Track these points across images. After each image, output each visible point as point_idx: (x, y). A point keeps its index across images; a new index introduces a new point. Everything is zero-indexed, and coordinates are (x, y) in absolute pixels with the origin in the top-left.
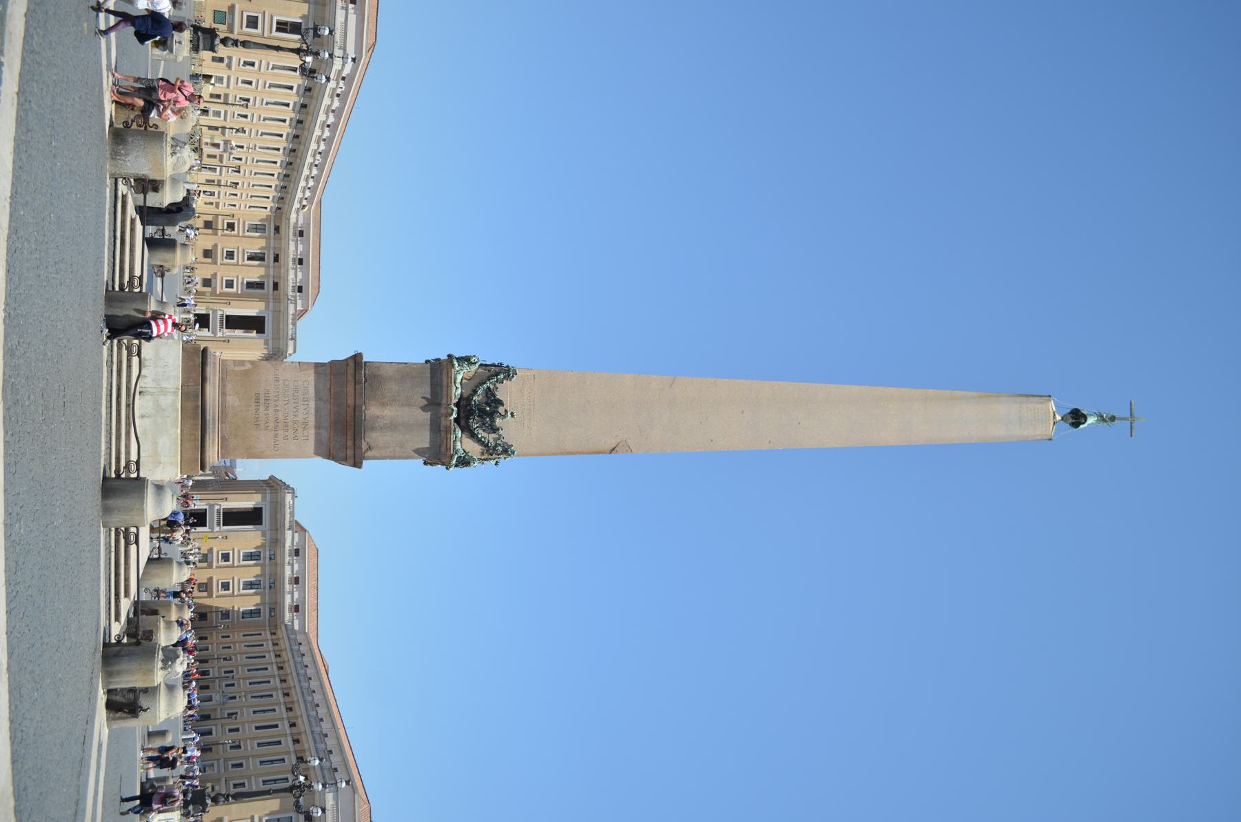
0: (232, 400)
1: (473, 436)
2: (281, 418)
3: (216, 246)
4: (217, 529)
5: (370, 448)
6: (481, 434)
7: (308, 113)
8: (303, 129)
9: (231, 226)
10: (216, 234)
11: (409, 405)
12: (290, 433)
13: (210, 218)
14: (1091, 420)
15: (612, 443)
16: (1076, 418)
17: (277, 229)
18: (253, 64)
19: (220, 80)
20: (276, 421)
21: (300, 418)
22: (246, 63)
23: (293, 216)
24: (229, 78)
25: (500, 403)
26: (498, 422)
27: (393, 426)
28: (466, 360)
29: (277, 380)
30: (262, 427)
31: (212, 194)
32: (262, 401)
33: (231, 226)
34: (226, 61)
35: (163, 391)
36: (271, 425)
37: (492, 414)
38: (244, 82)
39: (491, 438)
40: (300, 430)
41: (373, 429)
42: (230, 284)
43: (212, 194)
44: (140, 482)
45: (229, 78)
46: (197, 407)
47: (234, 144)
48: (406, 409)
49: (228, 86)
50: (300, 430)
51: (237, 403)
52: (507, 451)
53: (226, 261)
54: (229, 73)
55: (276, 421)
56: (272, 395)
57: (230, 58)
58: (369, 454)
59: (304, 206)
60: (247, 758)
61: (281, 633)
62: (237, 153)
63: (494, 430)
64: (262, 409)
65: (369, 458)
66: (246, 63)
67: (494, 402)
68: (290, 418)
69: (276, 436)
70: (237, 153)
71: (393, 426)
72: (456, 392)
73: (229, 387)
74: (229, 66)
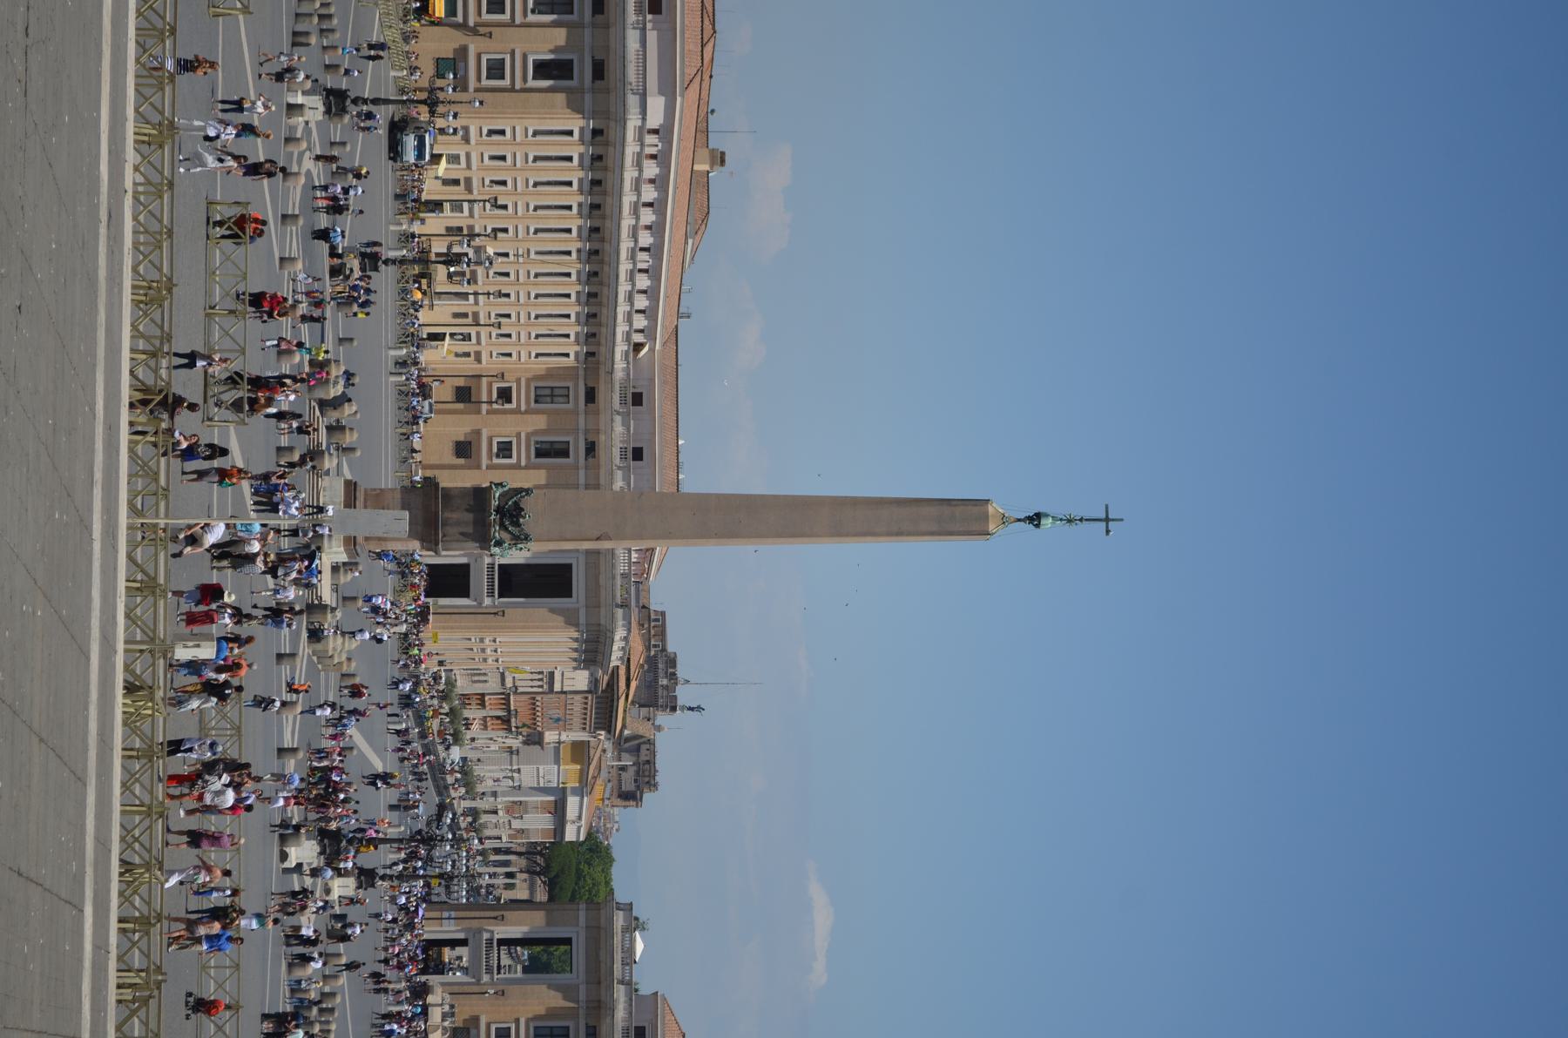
3: (478, 433)
4: (486, 978)
7: (605, 193)
8: (603, 217)
9: (505, 395)
10: (479, 412)
13: (461, 382)
15: (597, 534)
17: (591, 396)
18: (502, 132)
19: (454, 159)
22: (491, 132)
23: (620, 364)
24: (468, 156)
28: (501, 485)
31: (467, 337)
33: (505, 395)
38: (493, 158)
43: (467, 337)
45: (468, 156)
47: (490, 251)
49: (469, 167)
52: (527, 538)
53: (496, 461)
54: (467, 148)
57: (466, 129)
59: (638, 347)
62: (500, 265)
63: (518, 525)
66: (491, 132)
70: (500, 265)
72: (495, 503)
74: (466, 139)
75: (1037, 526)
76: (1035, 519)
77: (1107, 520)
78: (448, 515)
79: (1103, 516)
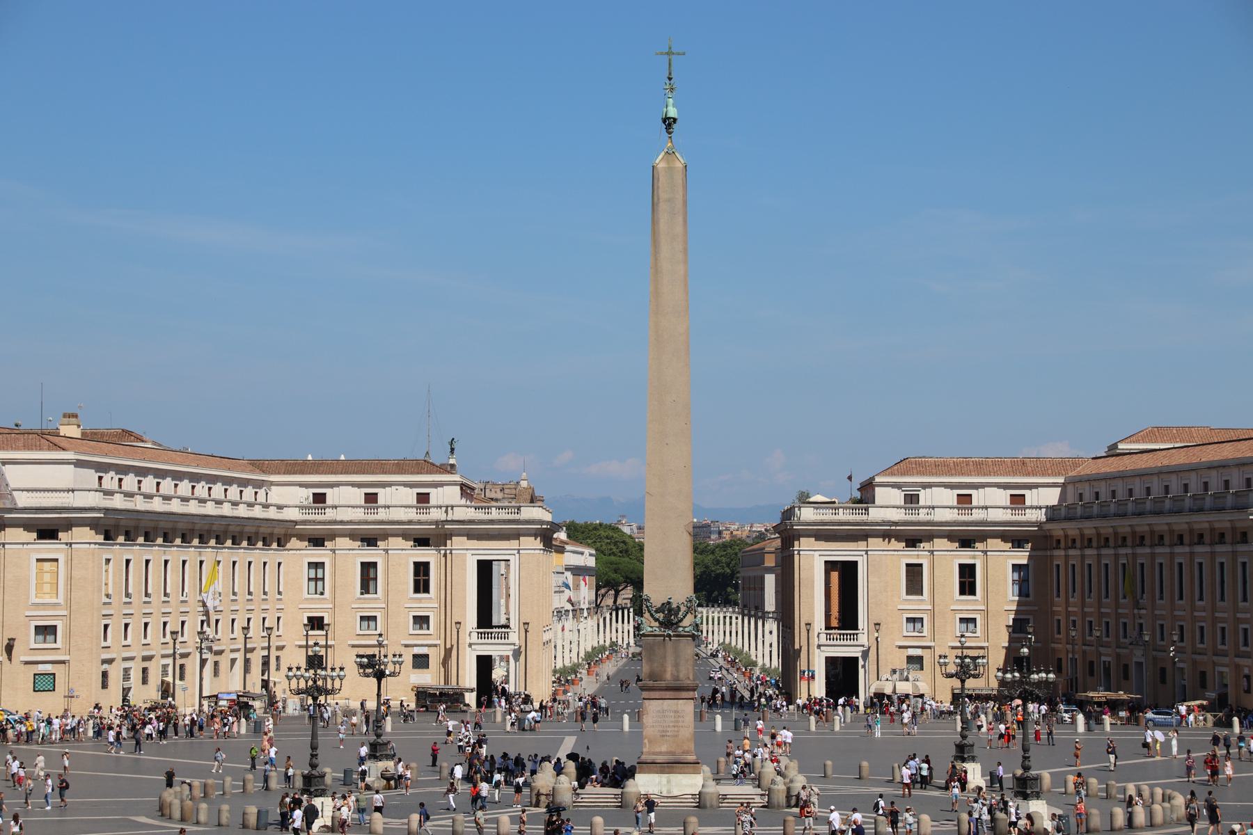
0: (664, 749)
1: (681, 620)
6: (680, 615)
14: (672, 112)
16: (669, 123)
26: (674, 606)
27: (676, 665)
34: (105, 666)
35: (660, 783)
37: (670, 610)
39: (683, 609)
42: (421, 621)
44: (700, 793)
49: (132, 659)
60: (1215, 620)
61: (1057, 529)
71: (676, 665)
73: (658, 750)
74: (110, 661)
75: (675, 120)
77: (669, 53)
78: (668, 676)
79: (666, 57)
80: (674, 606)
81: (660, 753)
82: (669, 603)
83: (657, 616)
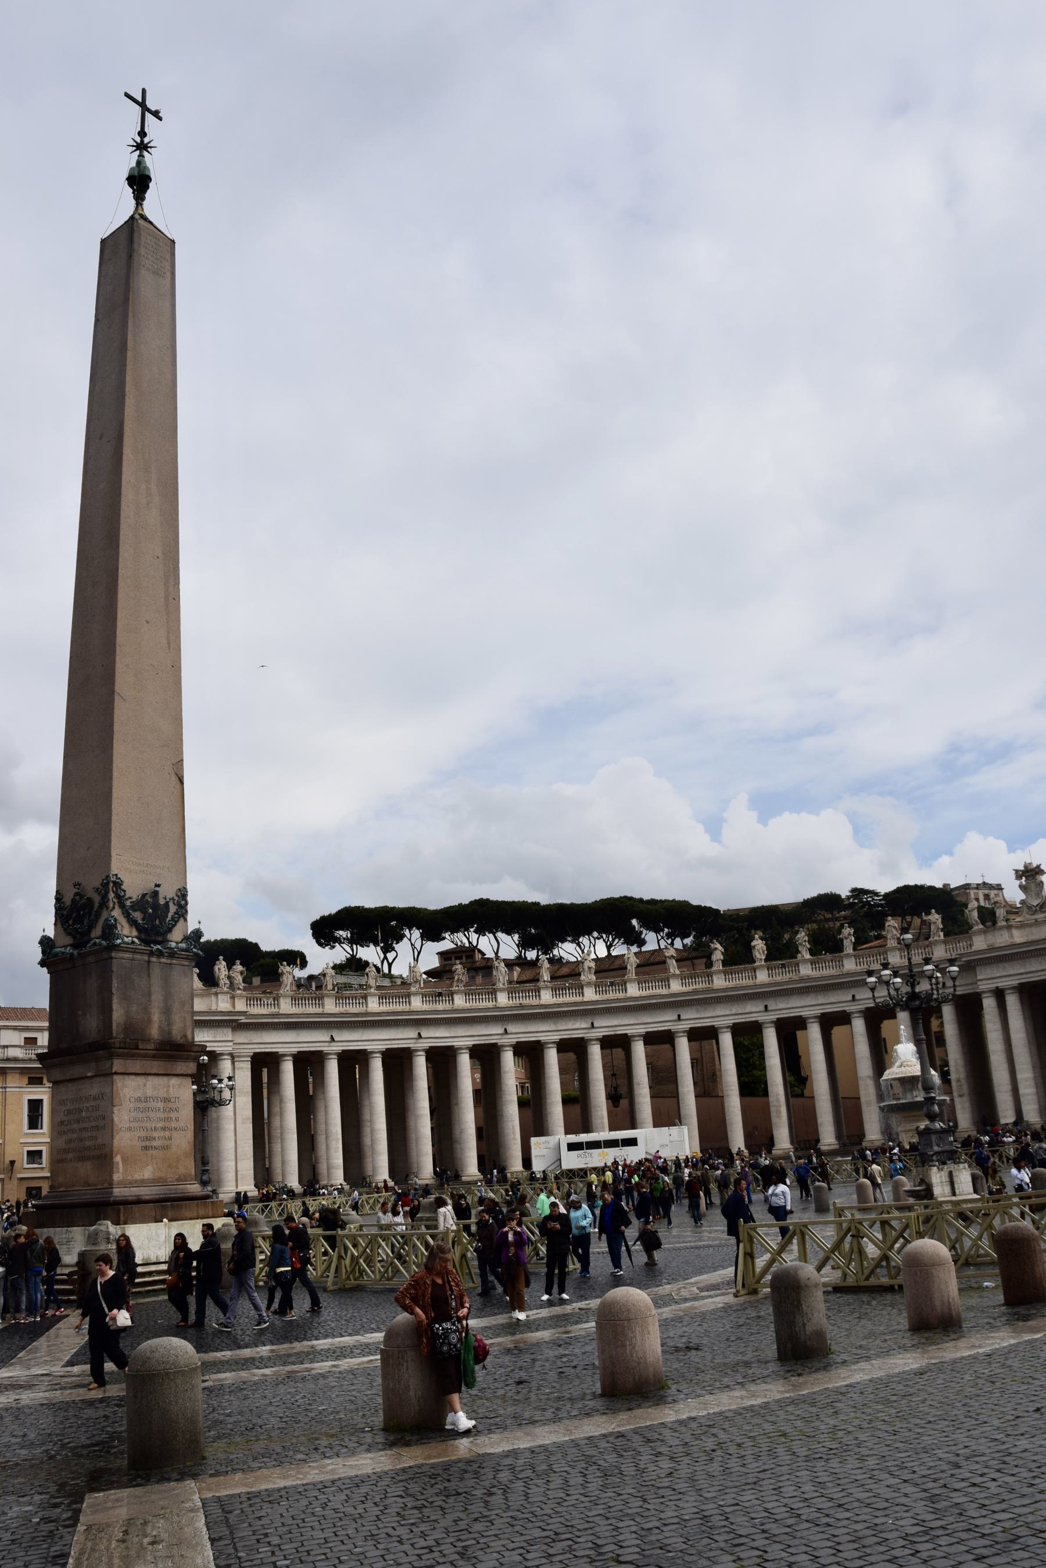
0: (147, 1173)
2: (160, 1125)
5: (185, 1036)
11: (150, 994)
12: (173, 1115)
15: (174, 778)
20: (164, 1129)
21: (160, 1105)
25: (144, 895)
26: (162, 902)
27: (167, 1012)
29: (130, 1129)
30: (168, 1143)
32: (148, 1143)
36: (167, 1134)
37: (156, 906)
40: (171, 1105)
41: (170, 1033)
46: (172, 1206)
48: (153, 997)
50: (171, 1105)
51: (150, 1168)
55: (164, 1129)
56: (143, 1134)
58: (190, 1037)
64: (154, 1144)
65: (193, 1038)
67: (141, 904)
68: (162, 1115)
69: (176, 1129)
71: (167, 1012)
73: (137, 1177)
76: (139, 182)
78: (155, 1032)
80: (162, 902)
81: (143, 1181)
82: (156, 894)
83: (138, 916)
